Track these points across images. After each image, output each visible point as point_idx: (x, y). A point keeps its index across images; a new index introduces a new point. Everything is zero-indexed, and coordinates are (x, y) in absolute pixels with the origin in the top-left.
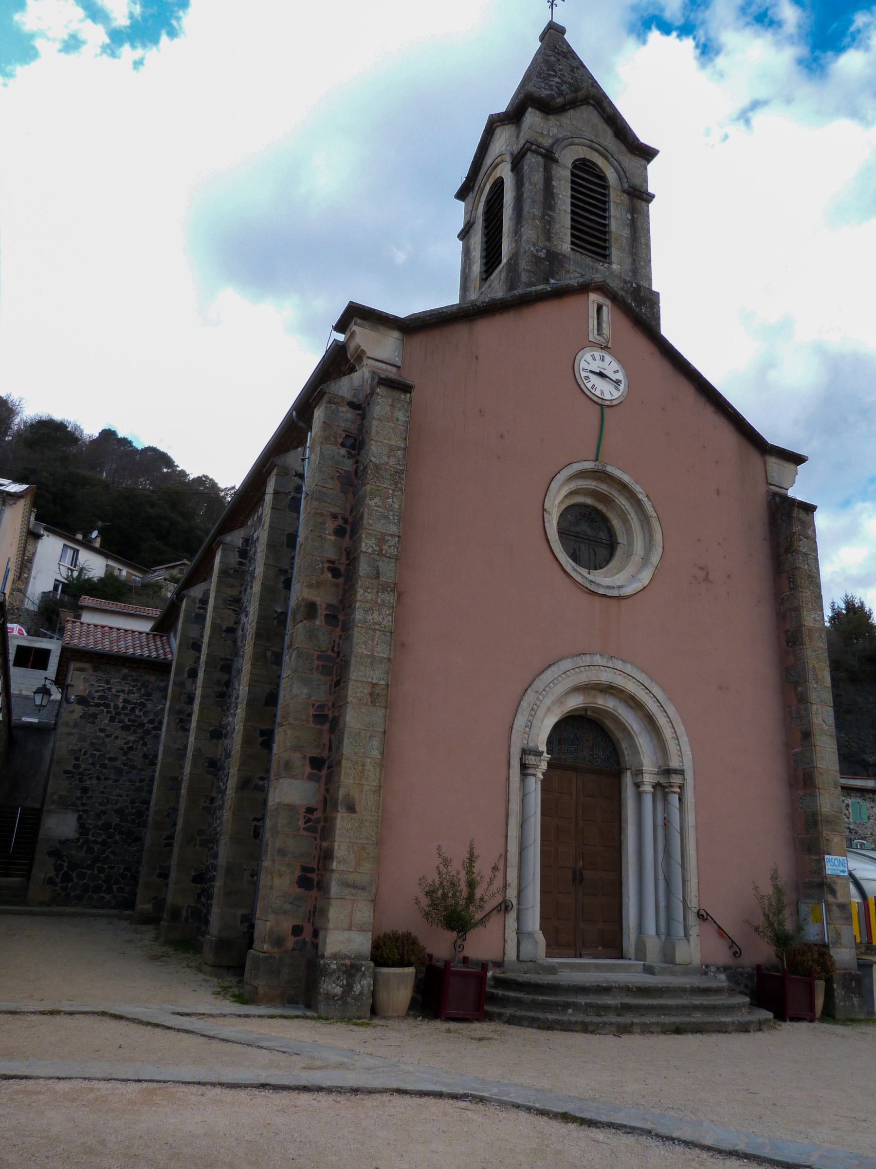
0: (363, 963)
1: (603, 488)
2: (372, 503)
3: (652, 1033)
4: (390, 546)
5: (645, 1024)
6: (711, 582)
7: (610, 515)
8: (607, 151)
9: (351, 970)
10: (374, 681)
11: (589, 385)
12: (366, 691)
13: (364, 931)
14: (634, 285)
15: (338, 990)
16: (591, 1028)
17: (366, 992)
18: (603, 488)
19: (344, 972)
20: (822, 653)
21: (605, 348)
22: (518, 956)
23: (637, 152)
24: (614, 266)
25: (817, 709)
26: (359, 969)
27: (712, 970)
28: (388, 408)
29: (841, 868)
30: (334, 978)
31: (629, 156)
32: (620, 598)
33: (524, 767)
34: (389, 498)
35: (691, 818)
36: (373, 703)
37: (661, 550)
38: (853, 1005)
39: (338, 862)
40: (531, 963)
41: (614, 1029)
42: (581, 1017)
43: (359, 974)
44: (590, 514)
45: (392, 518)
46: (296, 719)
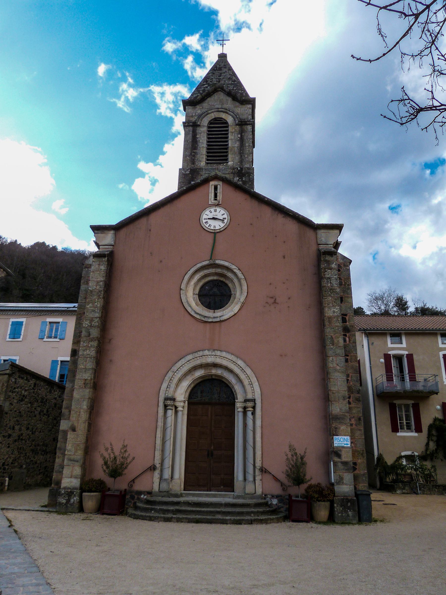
0: (75, 491)
1: (219, 270)
2: (88, 306)
3: (182, 522)
4: (95, 322)
5: (179, 518)
6: (277, 303)
7: (227, 282)
8: (226, 110)
9: (70, 493)
10: (86, 378)
11: (207, 226)
12: (82, 383)
13: (77, 478)
14: (239, 169)
15: (64, 501)
16: (152, 519)
17: (75, 502)
18: (219, 270)
19: (67, 494)
20: (338, 329)
21: (218, 205)
22: (159, 489)
23: (244, 103)
24: (229, 163)
25: (332, 359)
26: (73, 493)
27: (269, 497)
28: (97, 266)
29: (345, 443)
30: (63, 496)
31: (241, 106)
32: (221, 321)
33: (166, 406)
34: (96, 303)
35: (258, 423)
36: (85, 387)
37: (246, 294)
38: (348, 515)
39: (68, 451)
40: (165, 492)
41: (163, 519)
42: (157, 515)
43: (73, 495)
44: (218, 284)
45: (96, 310)
46: (67, 396)
